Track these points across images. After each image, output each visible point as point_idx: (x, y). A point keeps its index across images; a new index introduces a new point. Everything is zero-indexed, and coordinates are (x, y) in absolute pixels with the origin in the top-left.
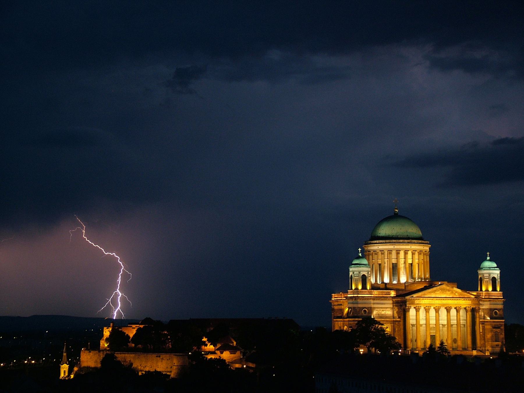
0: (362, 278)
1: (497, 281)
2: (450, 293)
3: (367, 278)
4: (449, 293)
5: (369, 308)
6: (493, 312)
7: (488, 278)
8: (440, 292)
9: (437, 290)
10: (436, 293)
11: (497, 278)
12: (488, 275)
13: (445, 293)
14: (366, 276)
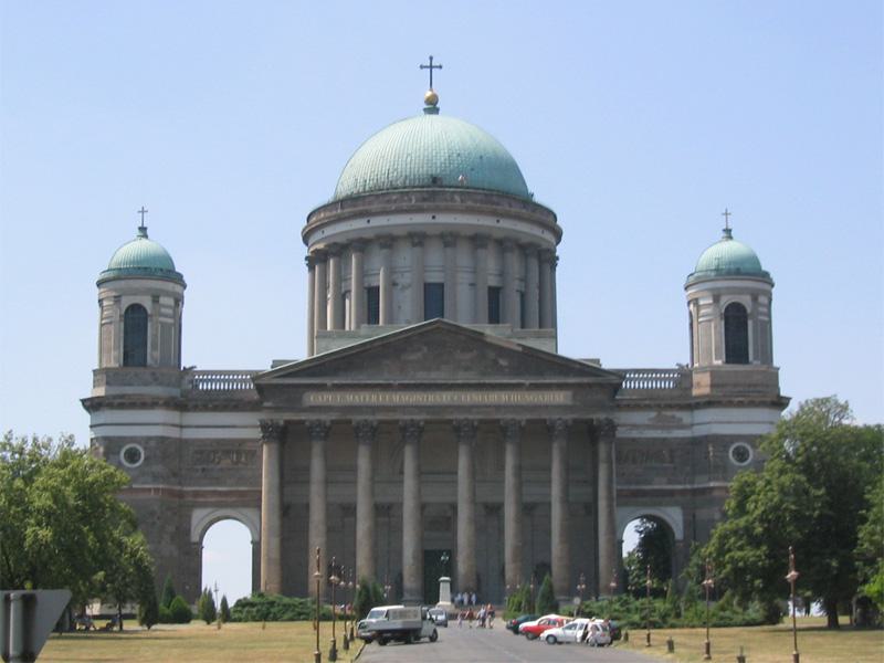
1: (750, 323)
6: (727, 452)
11: (749, 311)
14: (145, 310)
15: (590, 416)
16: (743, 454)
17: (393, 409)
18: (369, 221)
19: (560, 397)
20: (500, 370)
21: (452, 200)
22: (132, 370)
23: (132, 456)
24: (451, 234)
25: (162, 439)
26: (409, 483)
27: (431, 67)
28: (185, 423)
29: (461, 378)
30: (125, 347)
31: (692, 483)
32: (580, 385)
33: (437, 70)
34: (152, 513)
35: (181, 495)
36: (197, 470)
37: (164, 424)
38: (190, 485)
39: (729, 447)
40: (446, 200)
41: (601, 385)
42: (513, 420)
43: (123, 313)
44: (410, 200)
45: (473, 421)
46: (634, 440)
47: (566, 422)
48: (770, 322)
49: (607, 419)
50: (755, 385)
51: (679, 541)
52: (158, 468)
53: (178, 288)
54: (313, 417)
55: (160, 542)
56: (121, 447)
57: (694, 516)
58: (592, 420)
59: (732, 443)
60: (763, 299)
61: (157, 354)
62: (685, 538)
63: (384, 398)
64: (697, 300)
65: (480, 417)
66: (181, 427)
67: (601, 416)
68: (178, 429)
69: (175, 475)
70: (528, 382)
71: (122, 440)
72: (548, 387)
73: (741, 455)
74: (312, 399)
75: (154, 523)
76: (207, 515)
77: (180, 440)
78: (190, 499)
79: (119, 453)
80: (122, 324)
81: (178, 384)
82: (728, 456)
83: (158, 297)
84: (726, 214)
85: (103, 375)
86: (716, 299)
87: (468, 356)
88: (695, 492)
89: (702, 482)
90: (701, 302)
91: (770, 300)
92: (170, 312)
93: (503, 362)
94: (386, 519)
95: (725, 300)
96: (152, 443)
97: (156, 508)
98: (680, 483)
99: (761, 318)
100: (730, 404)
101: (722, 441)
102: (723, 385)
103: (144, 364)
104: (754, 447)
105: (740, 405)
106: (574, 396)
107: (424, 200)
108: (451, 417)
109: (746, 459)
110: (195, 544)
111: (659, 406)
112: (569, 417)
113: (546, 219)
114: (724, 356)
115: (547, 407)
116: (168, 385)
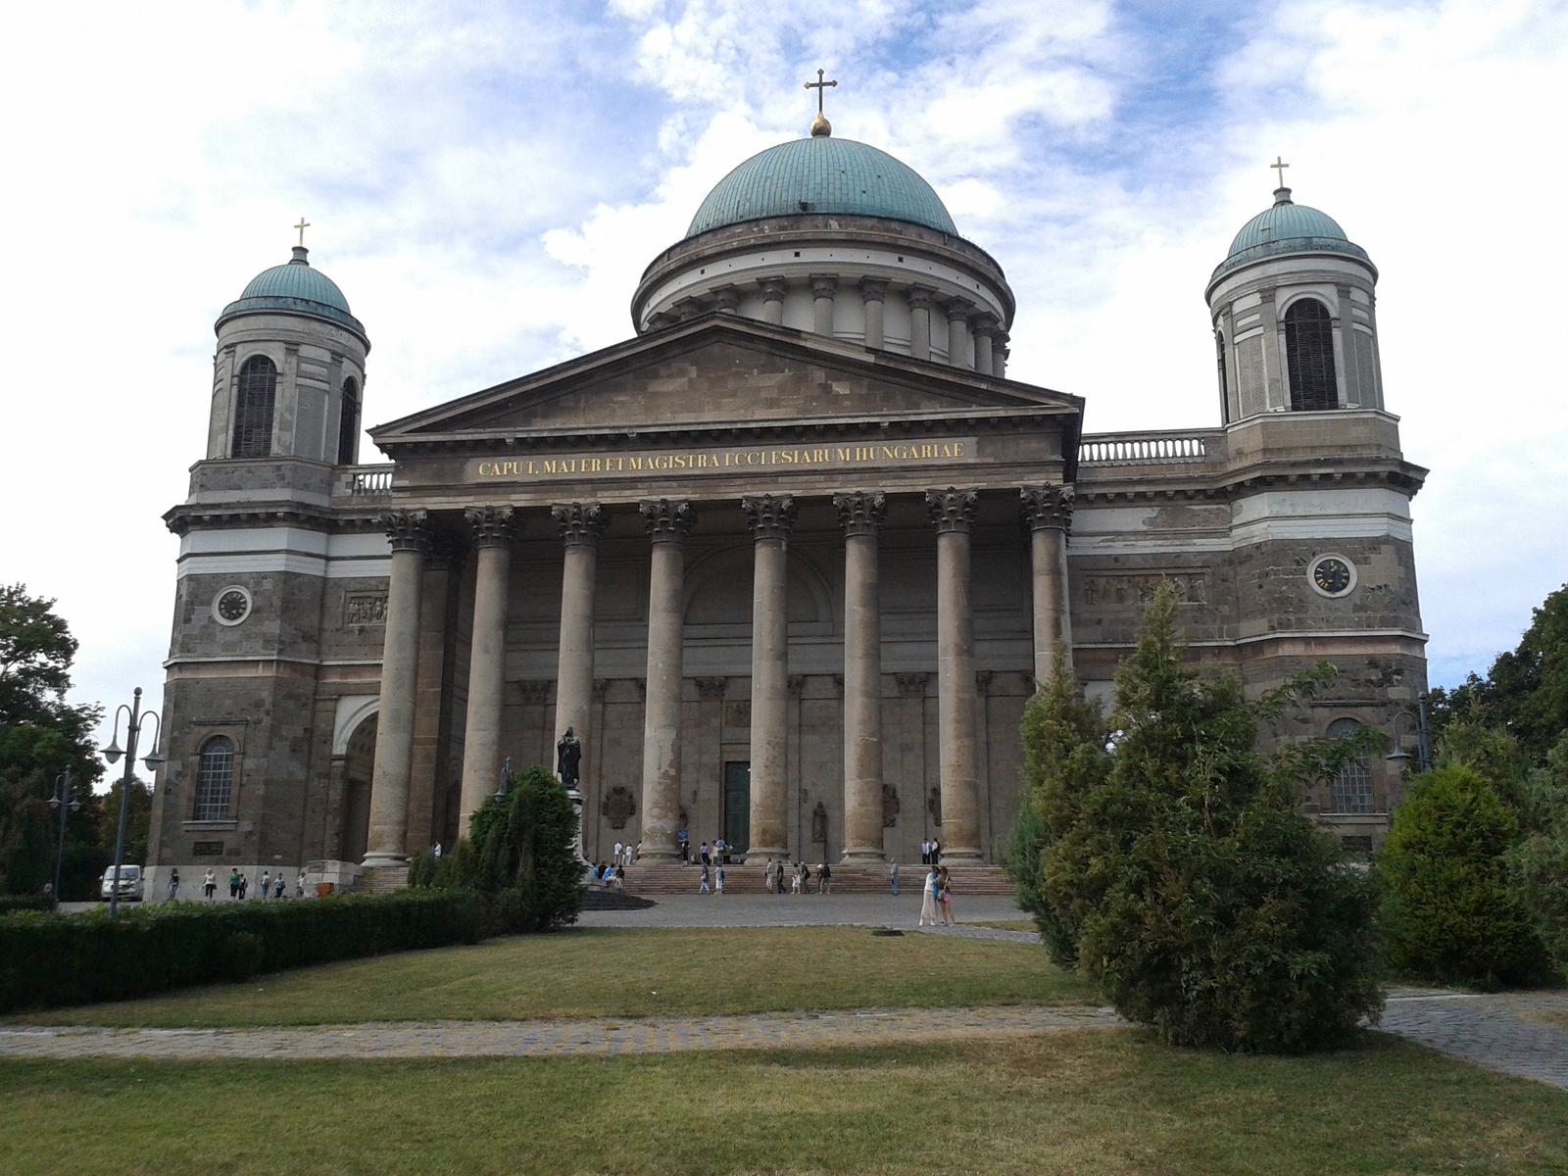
0: (242, 381)
1: (1337, 334)
2: (781, 388)
3: (278, 379)
4: (772, 383)
5: (264, 576)
8: (691, 381)
10: (650, 390)
11: (1333, 314)
12: (1254, 300)
13: (731, 384)
14: (274, 366)
15: (1015, 484)
17: (633, 482)
18: (703, 272)
19: (952, 450)
21: (826, 226)
22: (244, 465)
23: (232, 607)
24: (824, 278)
25: (287, 577)
26: (660, 623)
27: (821, 85)
29: (761, 416)
30: (238, 428)
34: (259, 704)
36: (352, 631)
37: (288, 552)
40: (817, 227)
42: (859, 494)
43: (237, 372)
44: (762, 230)
45: (779, 499)
46: (1116, 559)
47: (962, 494)
48: (1374, 337)
49: (1047, 487)
50: (1352, 447)
52: (273, 627)
53: (344, 338)
56: (215, 591)
58: (1017, 491)
59: (1314, 554)
60: (1357, 295)
61: (289, 437)
63: (614, 464)
64: (1231, 304)
65: (796, 493)
66: (328, 559)
68: (323, 561)
69: (307, 638)
70: (885, 422)
71: (218, 579)
73: (1334, 578)
74: (484, 469)
75: (259, 722)
76: (366, 705)
78: (333, 679)
79: (209, 603)
80: (235, 390)
81: (328, 487)
82: (1307, 583)
83: (298, 344)
84: (1280, 165)
85: (203, 474)
86: (1268, 295)
87: (776, 379)
90: (1237, 308)
91: (1372, 298)
93: (840, 388)
95: (1285, 298)
96: (267, 585)
98: (1212, 638)
99: (1356, 326)
101: (1292, 553)
102: (1290, 450)
103: (264, 452)
105: (1326, 482)
106: (980, 451)
107: (783, 228)
108: (739, 496)
110: (339, 758)
111: (1163, 494)
112: (969, 485)
113: (985, 270)
114: (1288, 396)
115: (926, 468)
116: (306, 487)
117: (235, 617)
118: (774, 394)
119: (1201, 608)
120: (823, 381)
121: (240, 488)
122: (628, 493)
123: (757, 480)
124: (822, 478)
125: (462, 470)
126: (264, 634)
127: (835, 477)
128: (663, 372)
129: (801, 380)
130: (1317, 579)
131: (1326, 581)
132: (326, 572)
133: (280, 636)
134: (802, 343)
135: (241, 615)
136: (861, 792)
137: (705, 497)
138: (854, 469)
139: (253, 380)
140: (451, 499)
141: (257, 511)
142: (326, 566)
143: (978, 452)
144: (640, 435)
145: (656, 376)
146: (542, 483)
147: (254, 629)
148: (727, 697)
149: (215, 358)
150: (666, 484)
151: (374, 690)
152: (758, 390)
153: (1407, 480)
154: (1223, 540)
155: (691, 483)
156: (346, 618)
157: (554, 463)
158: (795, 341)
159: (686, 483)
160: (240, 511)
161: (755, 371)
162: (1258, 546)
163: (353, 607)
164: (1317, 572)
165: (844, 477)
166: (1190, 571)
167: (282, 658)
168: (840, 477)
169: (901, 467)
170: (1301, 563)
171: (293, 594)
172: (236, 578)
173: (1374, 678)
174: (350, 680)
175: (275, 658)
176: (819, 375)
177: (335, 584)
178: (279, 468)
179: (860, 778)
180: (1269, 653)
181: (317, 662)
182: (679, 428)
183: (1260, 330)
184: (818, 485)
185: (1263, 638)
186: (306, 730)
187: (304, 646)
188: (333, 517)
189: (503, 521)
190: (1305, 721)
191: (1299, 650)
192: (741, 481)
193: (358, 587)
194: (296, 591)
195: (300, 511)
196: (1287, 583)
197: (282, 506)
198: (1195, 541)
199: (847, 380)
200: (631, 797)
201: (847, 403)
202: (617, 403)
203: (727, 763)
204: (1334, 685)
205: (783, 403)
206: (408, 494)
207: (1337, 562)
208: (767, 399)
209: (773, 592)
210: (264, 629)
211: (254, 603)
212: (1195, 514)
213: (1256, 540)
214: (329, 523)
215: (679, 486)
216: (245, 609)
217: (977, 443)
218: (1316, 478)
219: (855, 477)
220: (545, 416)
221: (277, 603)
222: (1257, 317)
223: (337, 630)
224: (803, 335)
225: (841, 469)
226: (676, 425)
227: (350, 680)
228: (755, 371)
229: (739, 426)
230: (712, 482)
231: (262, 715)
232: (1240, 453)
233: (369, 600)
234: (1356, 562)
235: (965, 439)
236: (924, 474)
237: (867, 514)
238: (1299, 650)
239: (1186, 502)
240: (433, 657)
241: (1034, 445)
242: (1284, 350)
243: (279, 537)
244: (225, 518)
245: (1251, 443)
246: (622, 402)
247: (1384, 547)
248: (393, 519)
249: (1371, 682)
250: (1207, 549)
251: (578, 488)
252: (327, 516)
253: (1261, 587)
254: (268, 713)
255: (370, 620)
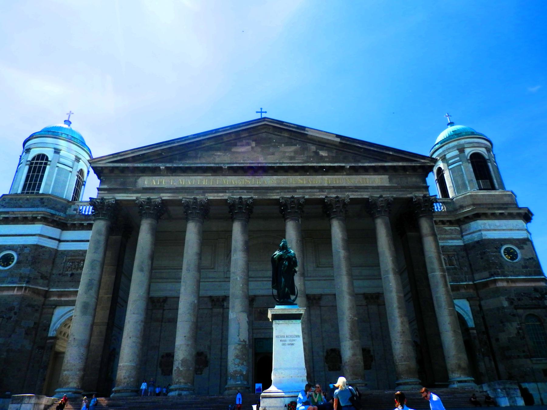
1: (489, 164)
5: (25, 246)
6: (500, 252)
7: (458, 158)
8: (252, 148)
9: (239, 144)
12: (456, 152)
13: (271, 150)
15: (409, 196)
16: (512, 253)
17: (224, 190)
20: (322, 159)
25: (37, 247)
28: (62, 239)
31: (473, 280)
32: (394, 168)
33: (265, 113)
34: (11, 309)
35: (47, 294)
36: (67, 275)
38: (57, 287)
39: (501, 249)
41: (414, 168)
43: (30, 158)
51: (472, 329)
54: (143, 197)
55: (10, 336)
57: (480, 306)
58: (412, 198)
59: (502, 245)
62: (475, 327)
64: (445, 155)
66: (60, 241)
67: (420, 194)
68: (57, 242)
69: (43, 277)
72: (366, 170)
74: (146, 181)
75: (10, 318)
77: (56, 253)
78: (55, 298)
82: (502, 256)
86: (462, 150)
87: (293, 148)
88: (476, 287)
89: (481, 277)
90: (448, 156)
91: (494, 155)
92: (70, 164)
93: (323, 153)
94: (221, 310)
95: (469, 151)
96: (26, 251)
97: (15, 304)
100: (494, 216)
101: (499, 243)
104: (520, 248)
105: (502, 216)
106: (390, 180)
109: (515, 259)
117: (7, 266)
118: (292, 154)
119: (455, 268)
120: (315, 150)
121: (21, 207)
122: (221, 194)
123: (286, 190)
124: (318, 190)
125: (136, 182)
126: (21, 274)
127: (324, 190)
128: (239, 144)
129: (304, 149)
130: (505, 255)
131: (509, 256)
132: (58, 247)
133: (29, 274)
134: (306, 133)
135: (10, 264)
136: (353, 348)
137: (261, 197)
138: (333, 187)
139: (36, 163)
140: (129, 195)
141: (28, 216)
142: (58, 244)
143: (390, 181)
144: (230, 168)
145: (236, 145)
146: (177, 189)
147: (16, 271)
148: (254, 306)
149: (21, 156)
150: (241, 191)
151: (73, 303)
152: (285, 152)
153: (527, 216)
154: (459, 241)
155: (253, 191)
156: (65, 270)
157: (184, 180)
158: (302, 132)
159: (250, 191)
160: (19, 216)
161: (283, 145)
162: (478, 242)
163: (69, 264)
164: (504, 252)
165: (328, 190)
166: (449, 253)
167: (30, 286)
168: (327, 190)
169: (355, 187)
170: (498, 249)
171: (39, 256)
172: (11, 248)
173: (538, 296)
174: (63, 299)
175: (24, 285)
176: (313, 148)
177: (62, 253)
178: (42, 199)
179: (352, 340)
180: (492, 286)
181: (47, 289)
182: (248, 165)
183: (461, 163)
184: (316, 194)
185: (488, 280)
186: (35, 323)
187: (41, 281)
188: (65, 222)
189: (156, 205)
190: (514, 315)
191: (505, 284)
192: (278, 191)
193: (73, 254)
194: (41, 254)
195: (49, 217)
196: (494, 256)
197: (40, 214)
198: (449, 241)
199: (326, 150)
200: (206, 357)
201: (328, 160)
202: (216, 155)
203: (255, 339)
204: (522, 299)
205: (297, 158)
206: (106, 192)
207: (512, 249)
208: (289, 156)
209: (297, 242)
210: (21, 271)
211: (18, 259)
212: (446, 231)
213: (476, 239)
214: (63, 226)
215: (247, 192)
216: (13, 262)
217: (389, 178)
218: (498, 214)
219: (333, 190)
220: (180, 160)
221: (30, 258)
222: (458, 158)
223: (60, 274)
224: (306, 129)
225: (327, 187)
226: (247, 163)
227: (63, 299)
228: (283, 145)
229: (278, 165)
230: (263, 191)
231: (12, 314)
232: (462, 207)
233: (77, 261)
234: (519, 248)
235: (383, 176)
236: (366, 190)
237: (341, 205)
238: (505, 284)
239: (442, 226)
240: (109, 279)
241: (414, 179)
242: (472, 170)
243: (37, 228)
244: (10, 219)
245: (466, 203)
246: (219, 155)
247: (527, 242)
248: (97, 203)
249: (537, 298)
250: (454, 244)
251: (196, 191)
252: (63, 221)
253: (482, 258)
254: (15, 313)
255: (77, 270)
